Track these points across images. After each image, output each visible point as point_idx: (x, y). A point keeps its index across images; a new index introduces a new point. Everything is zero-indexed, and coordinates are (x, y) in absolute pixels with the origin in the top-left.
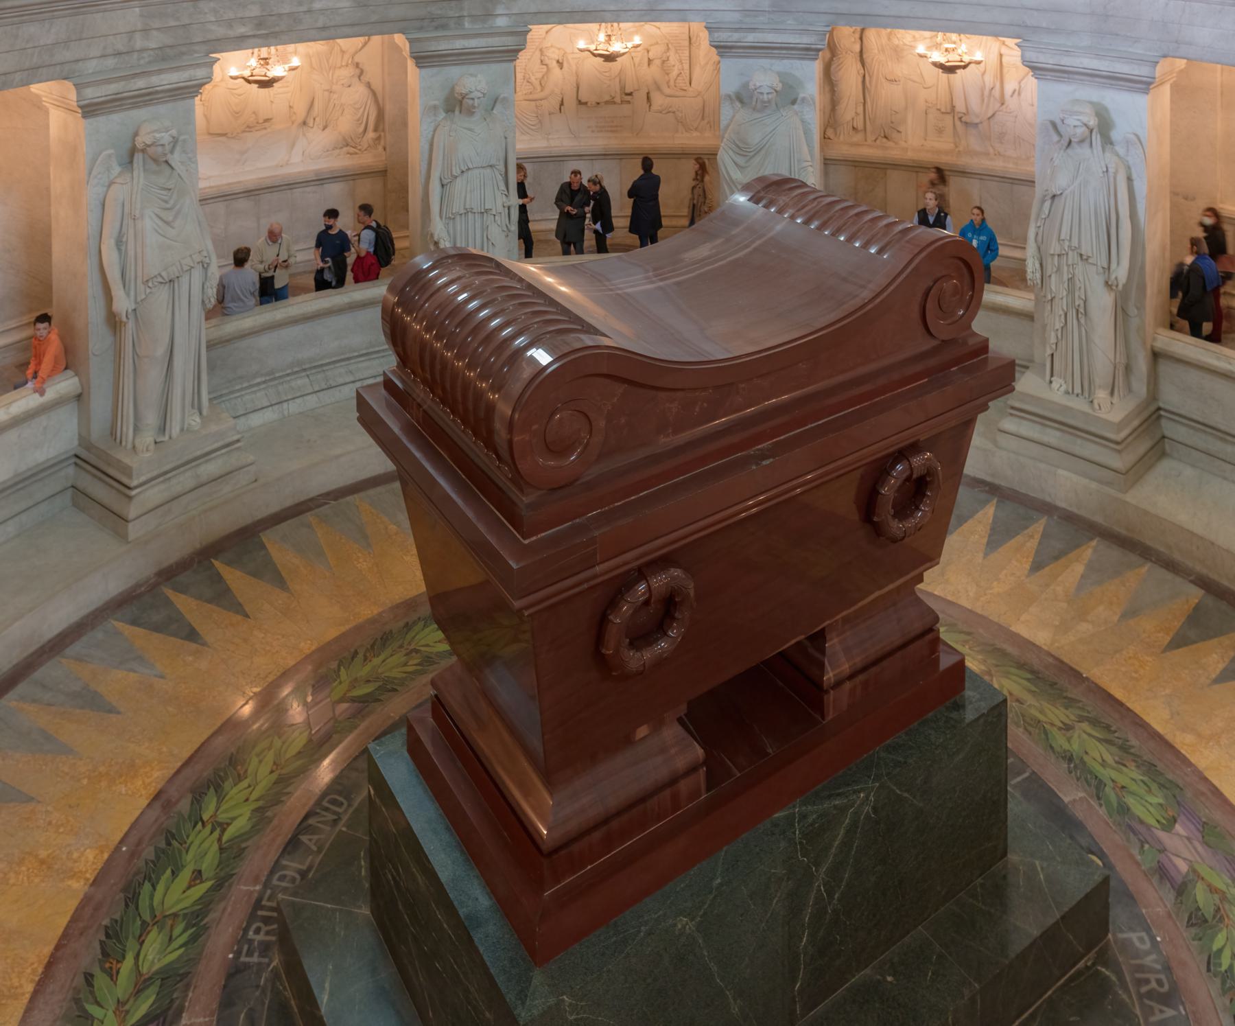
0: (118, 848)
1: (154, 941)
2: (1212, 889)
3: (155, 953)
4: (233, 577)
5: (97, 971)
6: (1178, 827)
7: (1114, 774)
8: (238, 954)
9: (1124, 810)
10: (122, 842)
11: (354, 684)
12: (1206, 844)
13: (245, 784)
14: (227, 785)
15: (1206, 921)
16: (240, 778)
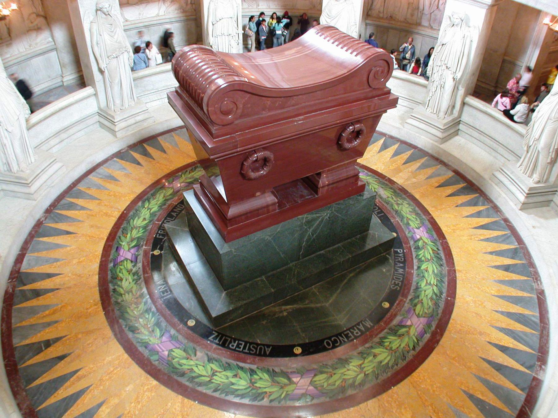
0: (123, 212)
1: (134, 232)
2: (424, 242)
3: (135, 234)
4: (150, 149)
5: (121, 236)
6: (421, 229)
7: (408, 216)
8: (156, 236)
9: (408, 224)
10: (125, 210)
11: (186, 179)
12: (427, 232)
13: (155, 200)
14: (151, 200)
15: (419, 248)
16: (154, 199)
